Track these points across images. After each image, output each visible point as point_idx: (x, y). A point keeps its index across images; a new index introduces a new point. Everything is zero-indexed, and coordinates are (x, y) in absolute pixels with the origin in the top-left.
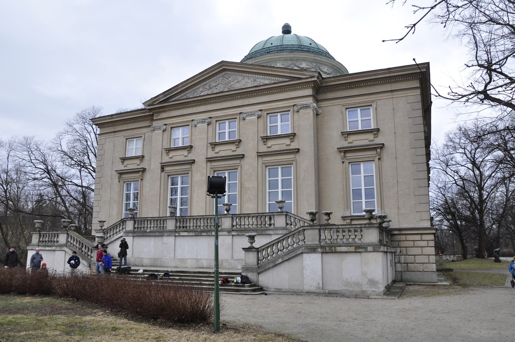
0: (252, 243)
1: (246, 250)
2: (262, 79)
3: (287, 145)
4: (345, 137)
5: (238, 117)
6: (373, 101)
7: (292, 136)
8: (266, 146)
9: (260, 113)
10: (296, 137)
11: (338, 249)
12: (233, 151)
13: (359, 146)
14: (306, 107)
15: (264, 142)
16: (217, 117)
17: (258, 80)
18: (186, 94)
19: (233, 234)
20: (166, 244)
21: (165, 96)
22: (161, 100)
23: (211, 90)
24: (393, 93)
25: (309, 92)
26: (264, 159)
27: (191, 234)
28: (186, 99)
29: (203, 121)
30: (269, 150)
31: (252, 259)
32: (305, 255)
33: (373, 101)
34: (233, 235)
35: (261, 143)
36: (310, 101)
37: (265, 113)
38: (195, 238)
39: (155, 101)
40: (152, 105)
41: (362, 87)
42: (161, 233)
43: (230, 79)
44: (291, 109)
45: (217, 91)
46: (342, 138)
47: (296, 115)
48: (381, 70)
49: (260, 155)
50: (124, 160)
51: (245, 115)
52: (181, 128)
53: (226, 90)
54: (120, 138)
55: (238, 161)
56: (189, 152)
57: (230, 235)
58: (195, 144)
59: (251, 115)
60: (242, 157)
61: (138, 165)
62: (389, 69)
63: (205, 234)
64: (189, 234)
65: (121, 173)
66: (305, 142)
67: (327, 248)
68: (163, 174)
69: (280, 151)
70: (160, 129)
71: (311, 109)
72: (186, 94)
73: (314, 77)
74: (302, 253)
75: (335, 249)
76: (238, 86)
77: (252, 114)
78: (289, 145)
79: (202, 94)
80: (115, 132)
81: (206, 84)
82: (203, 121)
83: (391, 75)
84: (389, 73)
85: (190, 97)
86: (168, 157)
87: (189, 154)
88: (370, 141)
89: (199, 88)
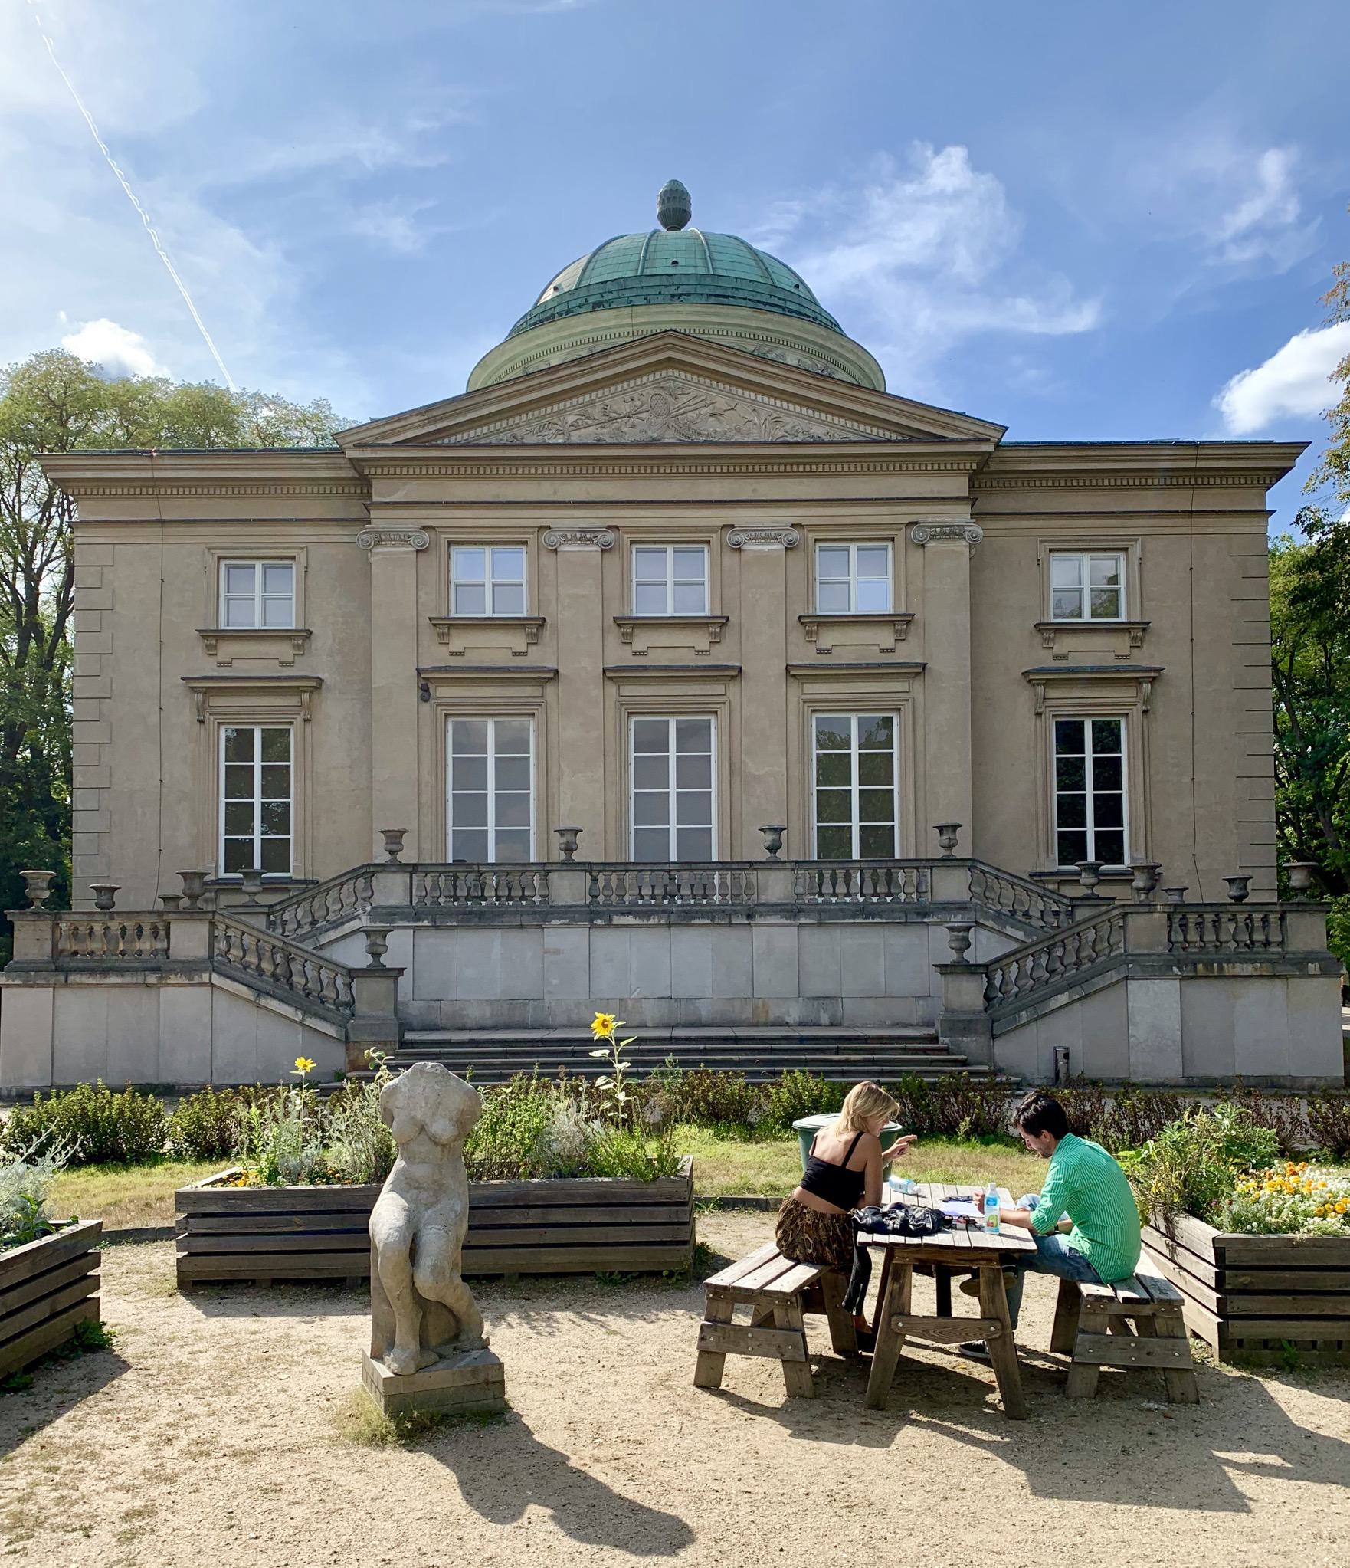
0: (960, 950)
1: (945, 969)
3: (883, 650)
4: (1048, 640)
5: (714, 538)
8: (813, 647)
9: (795, 534)
10: (912, 627)
11: (1228, 969)
12: (700, 653)
13: (1093, 670)
14: (952, 533)
15: (809, 633)
16: (637, 529)
19: (802, 920)
20: (557, 952)
25: (958, 485)
26: (809, 688)
28: (510, 445)
29: (586, 536)
30: (824, 659)
31: (969, 993)
32: (1133, 985)
34: (800, 925)
35: (798, 635)
36: (960, 515)
37: (811, 536)
38: (663, 932)
44: (900, 536)
45: (630, 436)
46: (1038, 638)
47: (916, 556)
49: (792, 673)
50: (213, 638)
51: (741, 537)
52: (488, 550)
54: (186, 555)
55: (719, 689)
58: (558, 614)
59: (767, 538)
65: (203, 689)
66: (944, 644)
67: (1200, 966)
68: (425, 707)
69: (868, 666)
71: (965, 543)
74: (1126, 978)
75: (1221, 968)
78: (891, 650)
82: (586, 536)
87: (533, 648)
88: (1118, 657)
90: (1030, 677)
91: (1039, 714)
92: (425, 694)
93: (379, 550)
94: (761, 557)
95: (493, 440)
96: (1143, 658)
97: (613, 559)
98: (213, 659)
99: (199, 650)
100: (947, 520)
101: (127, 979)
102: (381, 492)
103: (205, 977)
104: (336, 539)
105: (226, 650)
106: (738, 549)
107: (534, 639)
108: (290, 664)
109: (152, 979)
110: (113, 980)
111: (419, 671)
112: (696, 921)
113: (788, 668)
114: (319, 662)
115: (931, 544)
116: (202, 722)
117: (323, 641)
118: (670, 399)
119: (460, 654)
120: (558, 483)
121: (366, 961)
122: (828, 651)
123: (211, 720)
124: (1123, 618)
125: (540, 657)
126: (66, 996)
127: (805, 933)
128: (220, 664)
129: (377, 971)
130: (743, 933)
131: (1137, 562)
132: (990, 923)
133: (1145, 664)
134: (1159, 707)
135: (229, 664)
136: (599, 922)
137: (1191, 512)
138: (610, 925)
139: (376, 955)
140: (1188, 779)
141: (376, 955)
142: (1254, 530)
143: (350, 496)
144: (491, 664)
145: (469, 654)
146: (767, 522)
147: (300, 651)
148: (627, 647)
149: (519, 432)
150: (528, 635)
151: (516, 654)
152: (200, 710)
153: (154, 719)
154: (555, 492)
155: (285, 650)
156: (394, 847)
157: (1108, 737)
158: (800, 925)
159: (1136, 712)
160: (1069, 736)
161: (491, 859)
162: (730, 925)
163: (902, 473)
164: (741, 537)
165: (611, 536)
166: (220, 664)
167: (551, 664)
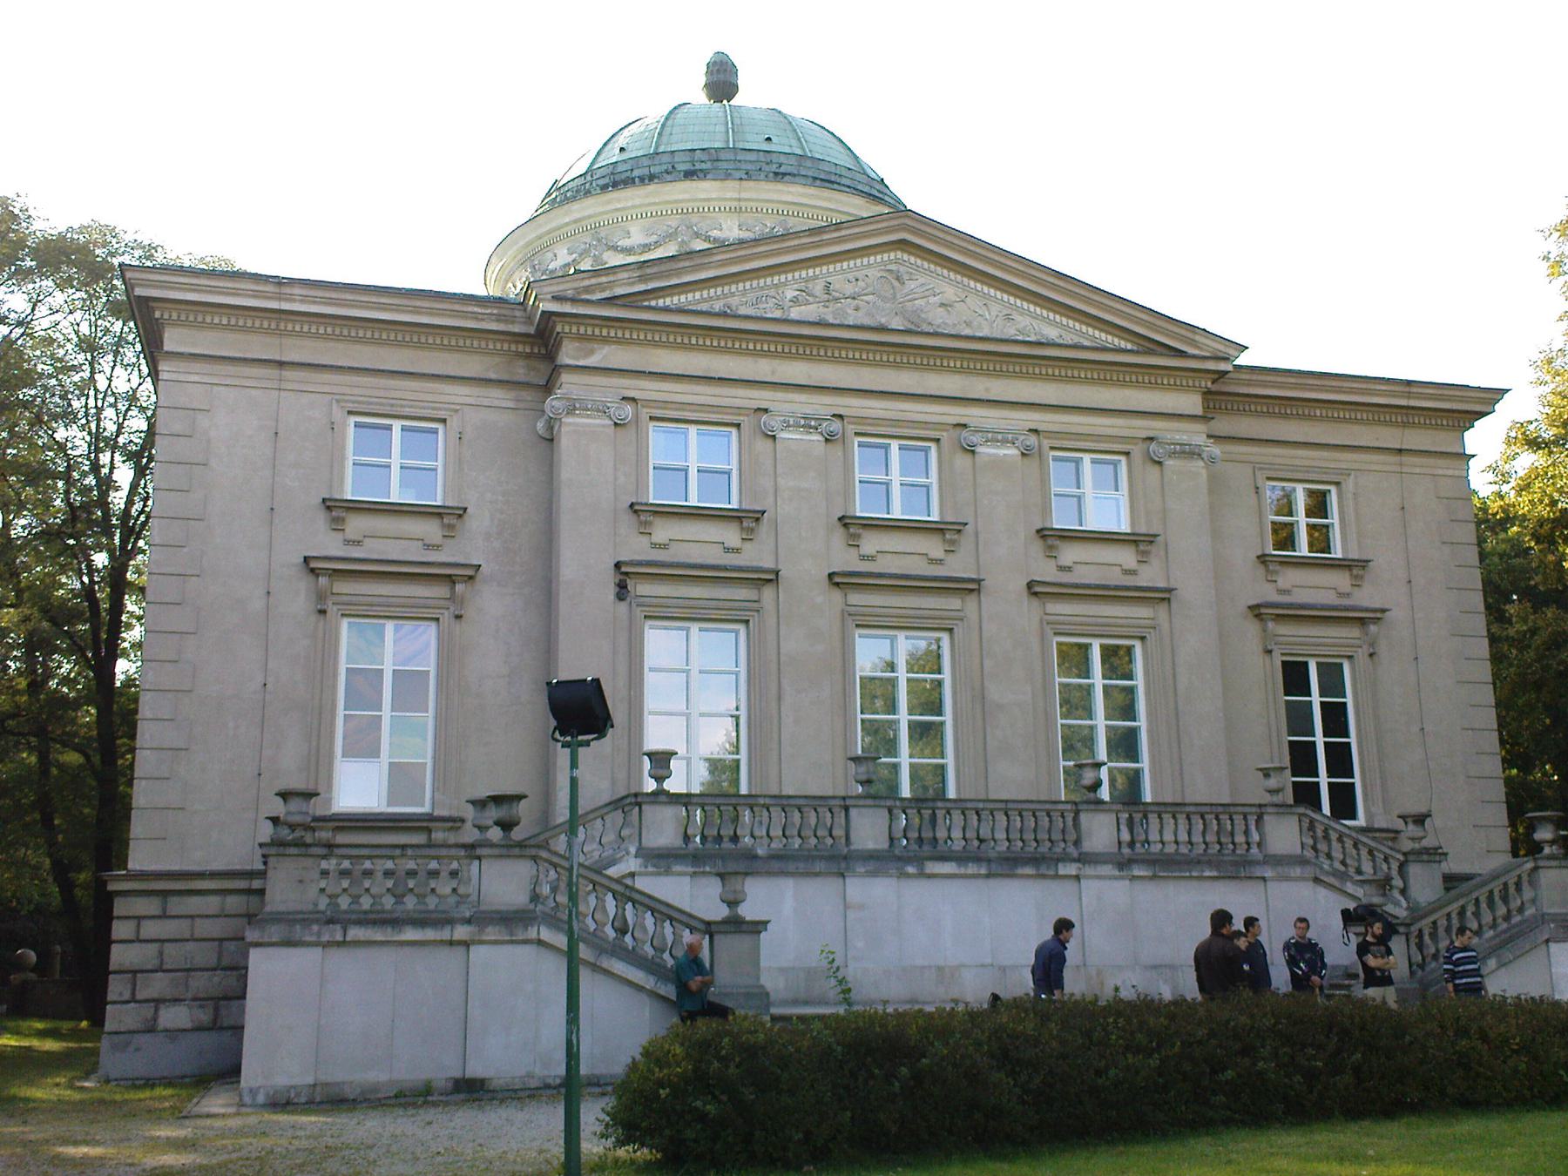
2: (1036, 317)
3: (1127, 572)
6: (1347, 472)
7: (1138, 541)
9: (1032, 440)
12: (933, 561)
14: (1192, 453)
17: (1019, 318)
18: (725, 296)
19: (1136, 872)
21: (642, 279)
22: (620, 291)
23: (833, 307)
24: (1406, 459)
25: (1191, 403)
27: (972, 869)
28: (723, 315)
29: (808, 423)
33: (1347, 472)
34: (1134, 878)
36: (1195, 435)
37: (1046, 443)
39: (587, 289)
40: (574, 301)
41: (1310, 417)
42: (839, 861)
43: (912, 285)
44: (1137, 451)
53: (896, 324)
55: (954, 603)
57: (1122, 878)
59: (1005, 441)
60: (970, 587)
61: (428, 547)
62: (1409, 383)
63: (1029, 870)
64: (962, 871)
68: (623, 607)
70: (604, 411)
72: (725, 296)
73: (1226, 359)
76: (939, 319)
79: (795, 313)
80: (281, 364)
81: (816, 277)
82: (808, 423)
83: (1413, 403)
84: (1409, 395)
85: (743, 311)
86: (644, 540)
87: (748, 545)
90: (1257, 611)
91: (1270, 652)
92: (622, 590)
93: (570, 420)
94: (997, 464)
95: (704, 307)
96: (1367, 597)
97: (837, 450)
98: (340, 535)
100: (1185, 438)
101: (430, 934)
102: (568, 354)
103: (532, 933)
104: (496, 403)
105: (357, 525)
108: (437, 547)
109: (461, 932)
110: (410, 934)
111: (618, 565)
112: (1020, 871)
113: (1030, 585)
114: (472, 547)
115: (1169, 463)
116: (323, 612)
117: (479, 521)
118: (896, 283)
119: (664, 546)
120: (777, 362)
121: (722, 912)
122: (1068, 569)
123: (332, 610)
124: (1337, 552)
125: (756, 555)
126: (339, 959)
127: (1138, 885)
128: (348, 542)
129: (736, 925)
130: (1070, 886)
131: (1350, 496)
132: (1331, 880)
133: (1366, 603)
134: (1382, 648)
135: (358, 543)
136: (911, 870)
137: (1400, 450)
138: (922, 875)
139: (733, 904)
140: (1415, 729)
141: (733, 904)
142: (1457, 473)
143: (518, 354)
144: (699, 561)
145: (674, 547)
146: (1003, 424)
147: (450, 532)
149: (734, 301)
150: (742, 529)
152: (321, 596)
153: (258, 604)
154: (773, 373)
155: (430, 529)
156: (661, 772)
157: (1332, 679)
158: (1134, 878)
159: (1361, 654)
160: (1295, 677)
161: (744, 790)
162: (1057, 876)
163: (1138, 385)
164: (975, 439)
165: (836, 426)
166: (348, 542)
167: (768, 563)
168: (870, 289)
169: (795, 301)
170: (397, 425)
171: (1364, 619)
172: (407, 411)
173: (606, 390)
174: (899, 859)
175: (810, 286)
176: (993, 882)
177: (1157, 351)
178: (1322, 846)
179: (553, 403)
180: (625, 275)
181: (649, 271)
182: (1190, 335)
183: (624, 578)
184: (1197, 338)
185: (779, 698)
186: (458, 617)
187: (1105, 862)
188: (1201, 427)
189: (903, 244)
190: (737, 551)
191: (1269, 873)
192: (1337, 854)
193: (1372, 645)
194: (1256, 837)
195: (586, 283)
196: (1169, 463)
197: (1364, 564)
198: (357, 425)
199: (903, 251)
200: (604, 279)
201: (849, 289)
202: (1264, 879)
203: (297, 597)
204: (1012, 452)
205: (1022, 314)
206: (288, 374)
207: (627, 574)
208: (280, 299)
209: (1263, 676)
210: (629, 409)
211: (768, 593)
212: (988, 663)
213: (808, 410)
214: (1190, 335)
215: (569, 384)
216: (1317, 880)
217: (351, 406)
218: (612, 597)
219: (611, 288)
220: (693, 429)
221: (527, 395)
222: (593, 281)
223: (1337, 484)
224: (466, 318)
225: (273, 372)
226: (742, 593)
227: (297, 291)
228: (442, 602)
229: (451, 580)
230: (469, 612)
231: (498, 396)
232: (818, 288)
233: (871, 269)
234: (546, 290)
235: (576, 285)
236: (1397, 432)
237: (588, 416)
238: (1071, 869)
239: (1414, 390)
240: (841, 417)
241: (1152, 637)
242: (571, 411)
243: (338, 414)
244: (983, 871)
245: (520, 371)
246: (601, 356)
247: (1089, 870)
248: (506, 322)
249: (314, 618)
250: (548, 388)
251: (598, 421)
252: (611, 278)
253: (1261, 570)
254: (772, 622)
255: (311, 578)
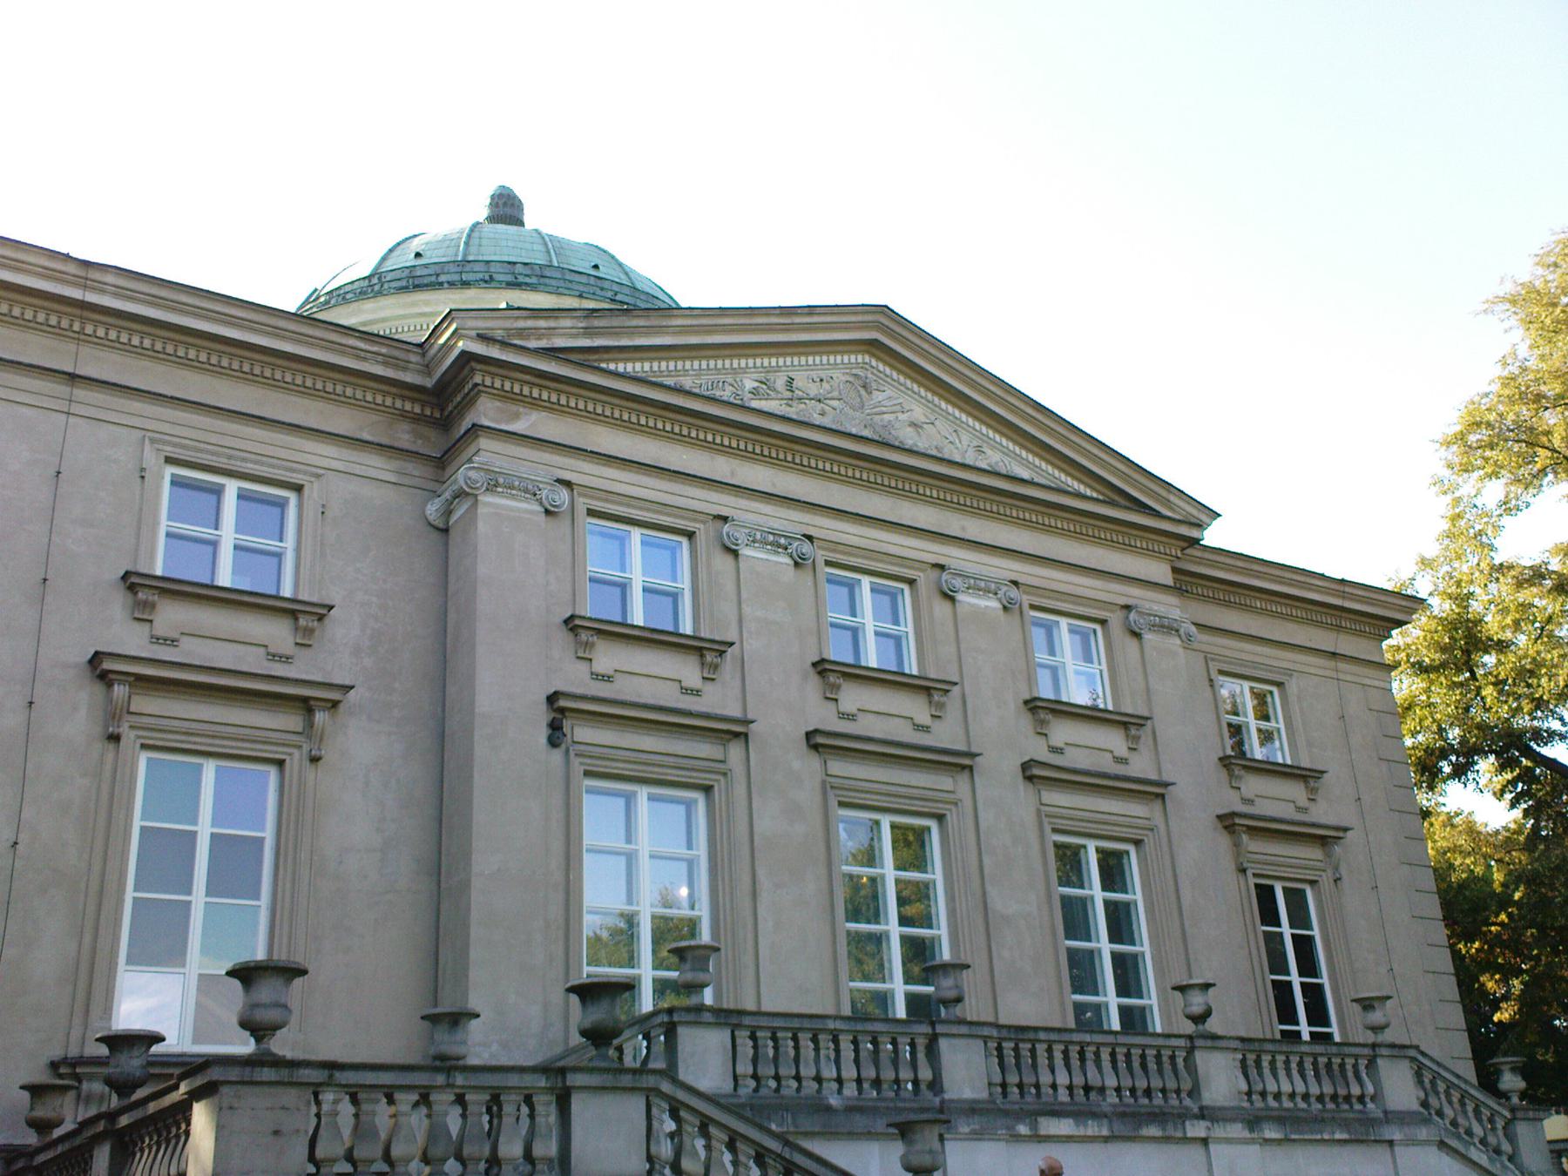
6: (1289, 672)
16: (835, 545)
17: (989, 452)
21: (589, 332)
22: (560, 342)
25: (1160, 571)
27: (1092, 1128)
29: (777, 542)
36: (1170, 607)
39: (521, 332)
40: (504, 344)
44: (1115, 618)
48: (1322, 576)
51: (958, 582)
55: (944, 782)
56: (711, 673)
57: (1252, 1141)
60: (960, 763)
61: (274, 657)
63: (1153, 1131)
68: (557, 756)
77: (982, 586)
80: (73, 378)
81: (778, 369)
82: (777, 542)
83: (1347, 604)
84: (1344, 595)
86: (583, 667)
89: (744, 370)
94: (979, 615)
96: (1323, 813)
97: (806, 577)
99: (118, 604)
106: (949, 597)
107: (711, 673)
108: (286, 659)
117: (344, 630)
119: (607, 678)
123: (129, 736)
125: (720, 700)
128: (156, 640)
130: (1197, 1152)
133: (1323, 820)
135: (172, 642)
136: (1023, 1129)
140: (1383, 970)
142: (1382, 684)
143: (404, 415)
144: (651, 701)
146: (985, 571)
148: (831, 705)
151: (686, 691)
152: (114, 714)
154: (733, 474)
155: (278, 633)
164: (958, 582)
166: (156, 640)
167: (734, 711)
168: (836, 394)
169: (755, 392)
170: (232, 487)
171: (1325, 839)
172: (250, 468)
173: (538, 466)
174: (1006, 1113)
175: (771, 376)
176: (1114, 1148)
177: (1134, 510)
178: (1433, 1101)
179: (463, 475)
180: (567, 323)
181: (596, 323)
182: (1164, 493)
183: (560, 713)
184: (1172, 498)
185: (754, 895)
186: (315, 760)
187: (1233, 1120)
188: (1172, 600)
189: (873, 346)
190: (696, 693)
191: (1396, 1135)
192: (1448, 1111)
193: (1336, 868)
194: (1370, 1089)
195: (521, 324)
196: (1148, 637)
197: (1317, 774)
198: (176, 482)
199: (873, 355)
200: (542, 323)
201: (814, 390)
202: (1391, 1143)
203: (75, 713)
204: (993, 604)
205: (993, 448)
206: (81, 393)
207: (562, 711)
208: (85, 287)
209: (1236, 896)
210: (563, 495)
211: (735, 751)
212: (987, 861)
213: (776, 524)
214: (1164, 493)
215: (489, 452)
216: (1442, 1145)
217: (169, 450)
218: (543, 740)
219: (549, 336)
220: (636, 534)
221: (415, 469)
222: (530, 323)
223: (1279, 685)
224: (343, 353)
225: (62, 389)
226: (704, 749)
227: (110, 279)
228: (294, 737)
229: (306, 706)
230: (329, 754)
231: (376, 465)
232: (780, 383)
233: (837, 369)
234: (470, 323)
235: (508, 324)
236: (1332, 635)
237: (513, 497)
238: (1197, 1129)
239: (1347, 589)
240: (810, 538)
241: (1149, 841)
242: (492, 487)
243: (151, 458)
244: (1105, 1132)
245: (404, 436)
246: (529, 422)
247: (1219, 1131)
248: (396, 367)
249: (98, 746)
250: (442, 463)
251: (524, 505)
252: (552, 323)
253: (1224, 774)
254: (740, 790)
255: (99, 688)
